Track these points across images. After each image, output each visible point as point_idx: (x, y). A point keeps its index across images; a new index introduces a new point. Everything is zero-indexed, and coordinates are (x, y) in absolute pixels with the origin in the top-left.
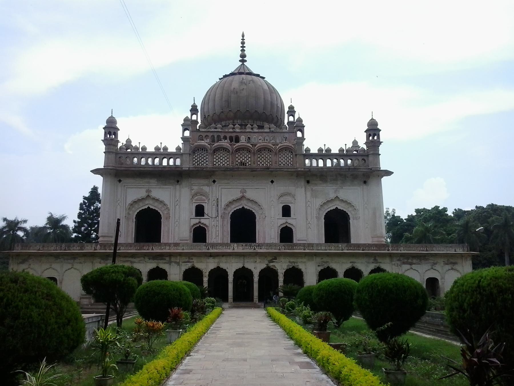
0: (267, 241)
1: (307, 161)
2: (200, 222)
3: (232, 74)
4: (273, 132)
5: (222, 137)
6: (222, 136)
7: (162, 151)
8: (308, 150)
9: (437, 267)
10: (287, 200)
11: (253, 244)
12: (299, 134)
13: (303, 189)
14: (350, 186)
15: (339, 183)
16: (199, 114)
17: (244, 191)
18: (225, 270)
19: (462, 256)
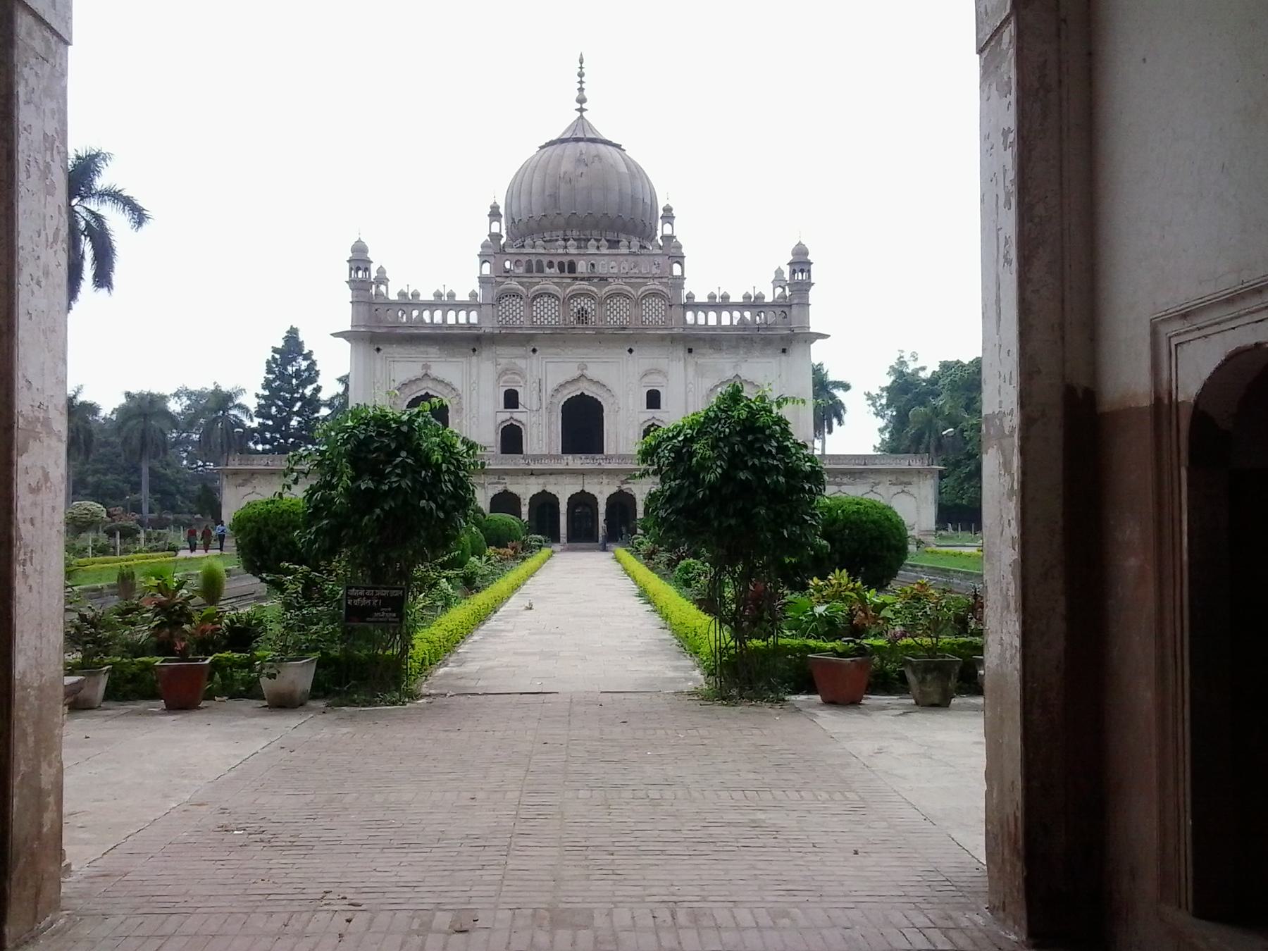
0: (622, 451)
1: (690, 316)
2: (511, 418)
3: (561, 141)
4: (634, 254)
5: (545, 263)
6: (545, 261)
7: (446, 299)
8: (690, 296)
9: (879, 489)
10: (655, 382)
11: (597, 456)
12: (677, 270)
13: (682, 362)
14: (758, 357)
15: (742, 352)
16: (503, 220)
17: (583, 367)
18: (554, 495)
19: (919, 472)
